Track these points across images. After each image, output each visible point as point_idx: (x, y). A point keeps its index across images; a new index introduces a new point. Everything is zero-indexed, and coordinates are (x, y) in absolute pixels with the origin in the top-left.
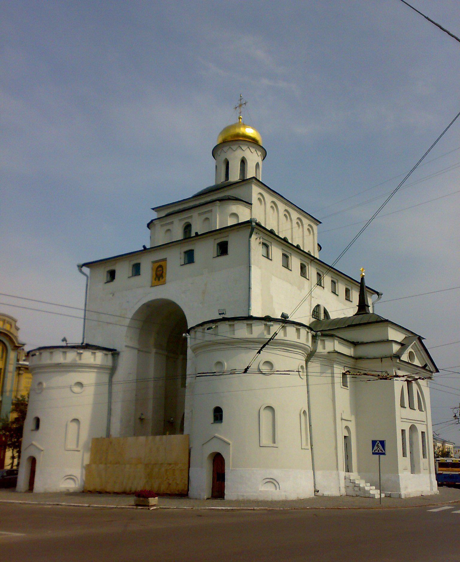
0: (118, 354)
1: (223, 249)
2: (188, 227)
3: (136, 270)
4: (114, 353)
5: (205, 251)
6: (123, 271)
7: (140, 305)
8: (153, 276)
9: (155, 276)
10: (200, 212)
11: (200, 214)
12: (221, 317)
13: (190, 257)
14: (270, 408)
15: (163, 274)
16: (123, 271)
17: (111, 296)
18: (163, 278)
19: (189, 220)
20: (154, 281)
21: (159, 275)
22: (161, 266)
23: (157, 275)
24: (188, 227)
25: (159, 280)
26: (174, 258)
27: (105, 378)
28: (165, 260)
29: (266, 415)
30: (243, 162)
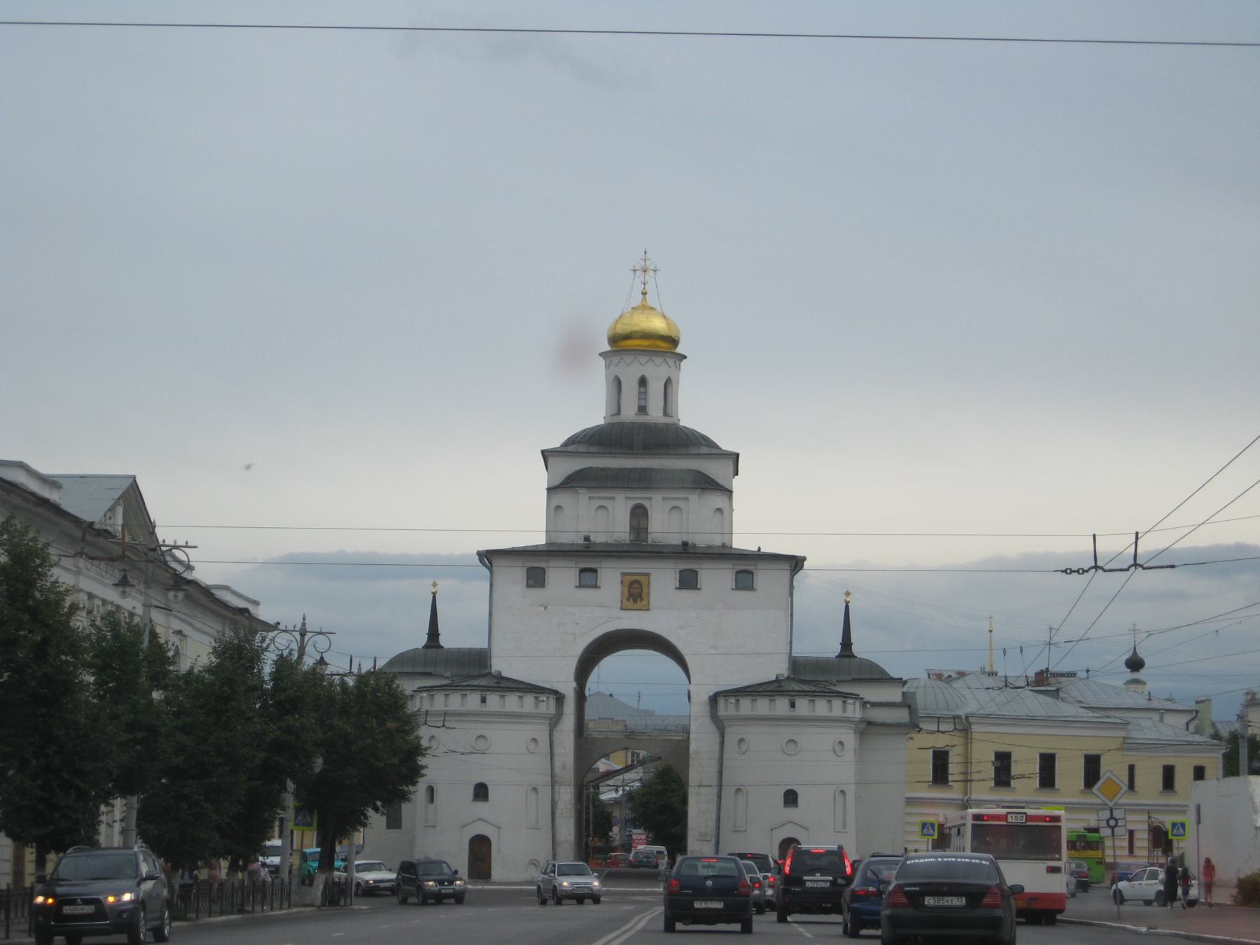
1: (744, 581)
2: (639, 514)
4: (559, 698)
5: (716, 579)
6: (562, 577)
7: (600, 632)
8: (622, 594)
10: (667, 496)
11: (664, 499)
13: (688, 581)
14: (843, 792)
16: (562, 577)
17: (542, 609)
18: (642, 600)
19: (646, 503)
21: (636, 594)
23: (631, 595)
24: (639, 514)
26: (662, 578)
27: (547, 728)
28: (648, 575)
29: (839, 798)
30: (668, 383)
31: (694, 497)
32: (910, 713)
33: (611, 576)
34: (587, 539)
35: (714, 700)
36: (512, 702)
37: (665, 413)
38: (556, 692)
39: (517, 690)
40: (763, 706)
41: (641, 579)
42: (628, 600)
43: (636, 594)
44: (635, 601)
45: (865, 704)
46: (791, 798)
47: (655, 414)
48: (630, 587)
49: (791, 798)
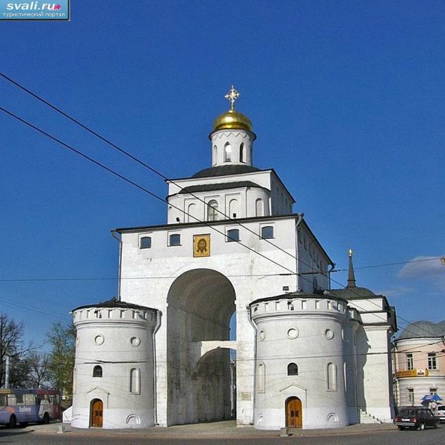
0: (161, 314)
1: (267, 234)
3: (175, 241)
4: (154, 312)
9: (197, 248)
12: (284, 293)
13: (233, 237)
15: (207, 248)
18: (206, 250)
20: (196, 253)
21: (202, 247)
22: (203, 240)
23: (199, 248)
25: (202, 252)
26: (217, 235)
31: (243, 191)
32: (389, 316)
33: (186, 235)
34: (178, 220)
35: (249, 308)
36: (115, 313)
37: (241, 161)
38: (155, 310)
39: (122, 307)
40: (271, 307)
41: (205, 238)
42: (198, 251)
43: (202, 247)
44: (202, 252)
45: (358, 313)
46: (293, 370)
47: (235, 161)
48: (199, 243)
49: (293, 370)
